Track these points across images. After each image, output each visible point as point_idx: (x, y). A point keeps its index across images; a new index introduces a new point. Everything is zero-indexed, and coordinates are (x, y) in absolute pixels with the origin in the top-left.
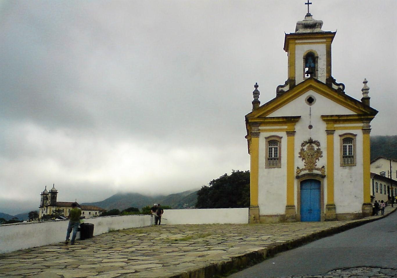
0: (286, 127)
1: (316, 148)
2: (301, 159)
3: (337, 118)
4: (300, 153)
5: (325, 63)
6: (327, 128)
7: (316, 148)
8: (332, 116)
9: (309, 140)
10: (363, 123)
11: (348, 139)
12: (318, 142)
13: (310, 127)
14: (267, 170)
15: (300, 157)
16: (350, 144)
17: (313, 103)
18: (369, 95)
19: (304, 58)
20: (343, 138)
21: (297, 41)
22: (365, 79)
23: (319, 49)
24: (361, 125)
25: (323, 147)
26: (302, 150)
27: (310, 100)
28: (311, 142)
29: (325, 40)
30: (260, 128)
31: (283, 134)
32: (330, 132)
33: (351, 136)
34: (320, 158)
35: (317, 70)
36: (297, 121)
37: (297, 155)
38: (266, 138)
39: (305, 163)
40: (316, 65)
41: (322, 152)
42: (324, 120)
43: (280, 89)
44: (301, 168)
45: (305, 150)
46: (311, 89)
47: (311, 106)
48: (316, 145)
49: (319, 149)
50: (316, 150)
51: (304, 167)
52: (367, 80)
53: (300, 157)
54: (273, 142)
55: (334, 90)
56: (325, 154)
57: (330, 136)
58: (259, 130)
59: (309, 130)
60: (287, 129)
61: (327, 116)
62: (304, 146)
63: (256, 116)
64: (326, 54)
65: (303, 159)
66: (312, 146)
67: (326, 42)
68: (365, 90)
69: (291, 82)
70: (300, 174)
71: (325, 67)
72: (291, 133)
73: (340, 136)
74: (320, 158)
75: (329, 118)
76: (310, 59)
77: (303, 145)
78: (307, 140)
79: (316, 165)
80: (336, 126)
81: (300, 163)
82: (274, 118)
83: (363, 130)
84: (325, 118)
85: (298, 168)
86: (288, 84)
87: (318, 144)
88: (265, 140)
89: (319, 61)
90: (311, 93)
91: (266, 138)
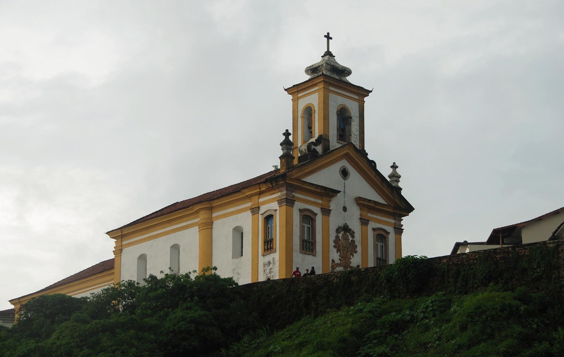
0: (320, 202)
1: (350, 239)
2: (335, 250)
3: (373, 205)
4: (335, 242)
5: (358, 128)
6: (361, 215)
7: (350, 239)
8: (370, 201)
9: (344, 226)
10: (395, 219)
11: (381, 236)
12: (353, 232)
13: (345, 209)
14: (300, 255)
15: (334, 246)
16: (381, 244)
17: (347, 177)
18: (400, 185)
19: (337, 114)
20: (376, 233)
21: (331, 88)
22: (394, 163)
23: (352, 107)
24: (393, 221)
25: (358, 238)
26: (337, 237)
27: (344, 173)
28: (345, 229)
29: (357, 97)
30: (294, 194)
31: (316, 210)
32: (364, 222)
33: (384, 234)
34: (354, 254)
35: (351, 135)
36: (333, 196)
37: (332, 244)
38: (301, 211)
39: (340, 256)
40: (347, 128)
41: (356, 247)
42: (358, 204)
43: (313, 147)
44: (336, 262)
45: (340, 238)
46: (346, 159)
47: (346, 181)
48: (351, 235)
49: (353, 241)
50: (350, 241)
51: (339, 262)
52: (397, 164)
53: (334, 246)
54: (308, 218)
55: (368, 169)
56: (359, 249)
57: (364, 227)
58: (294, 196)
59: (343, 212)
60: (322, 205)
61: (365, 200)
62: (340, 232)
63: (294, 177)
64: (358, 116)
65: (338, 251)
66: (348, 236)
67: (358, 100)
68: (395, 177)
69: (323, 140)
70: (335, 270)
71: (358, 133)
72: (326, 212)
73: (374, 229)
74: (354, 254)
75: (365, 203)
76: (344, 117)
77: (338, 231)
78: (341, 225)
79: (351, 263)
80: (369, 215)
81: (335, 256)
82: (312, 184)
83: (395, 228)
84: (362, 202)
85: (333, 261)
86: (320, 143)
87: (352, 234)
88: (298, 213)
89: (352, 123)
90: (344, 163)
91: (301, 211)
